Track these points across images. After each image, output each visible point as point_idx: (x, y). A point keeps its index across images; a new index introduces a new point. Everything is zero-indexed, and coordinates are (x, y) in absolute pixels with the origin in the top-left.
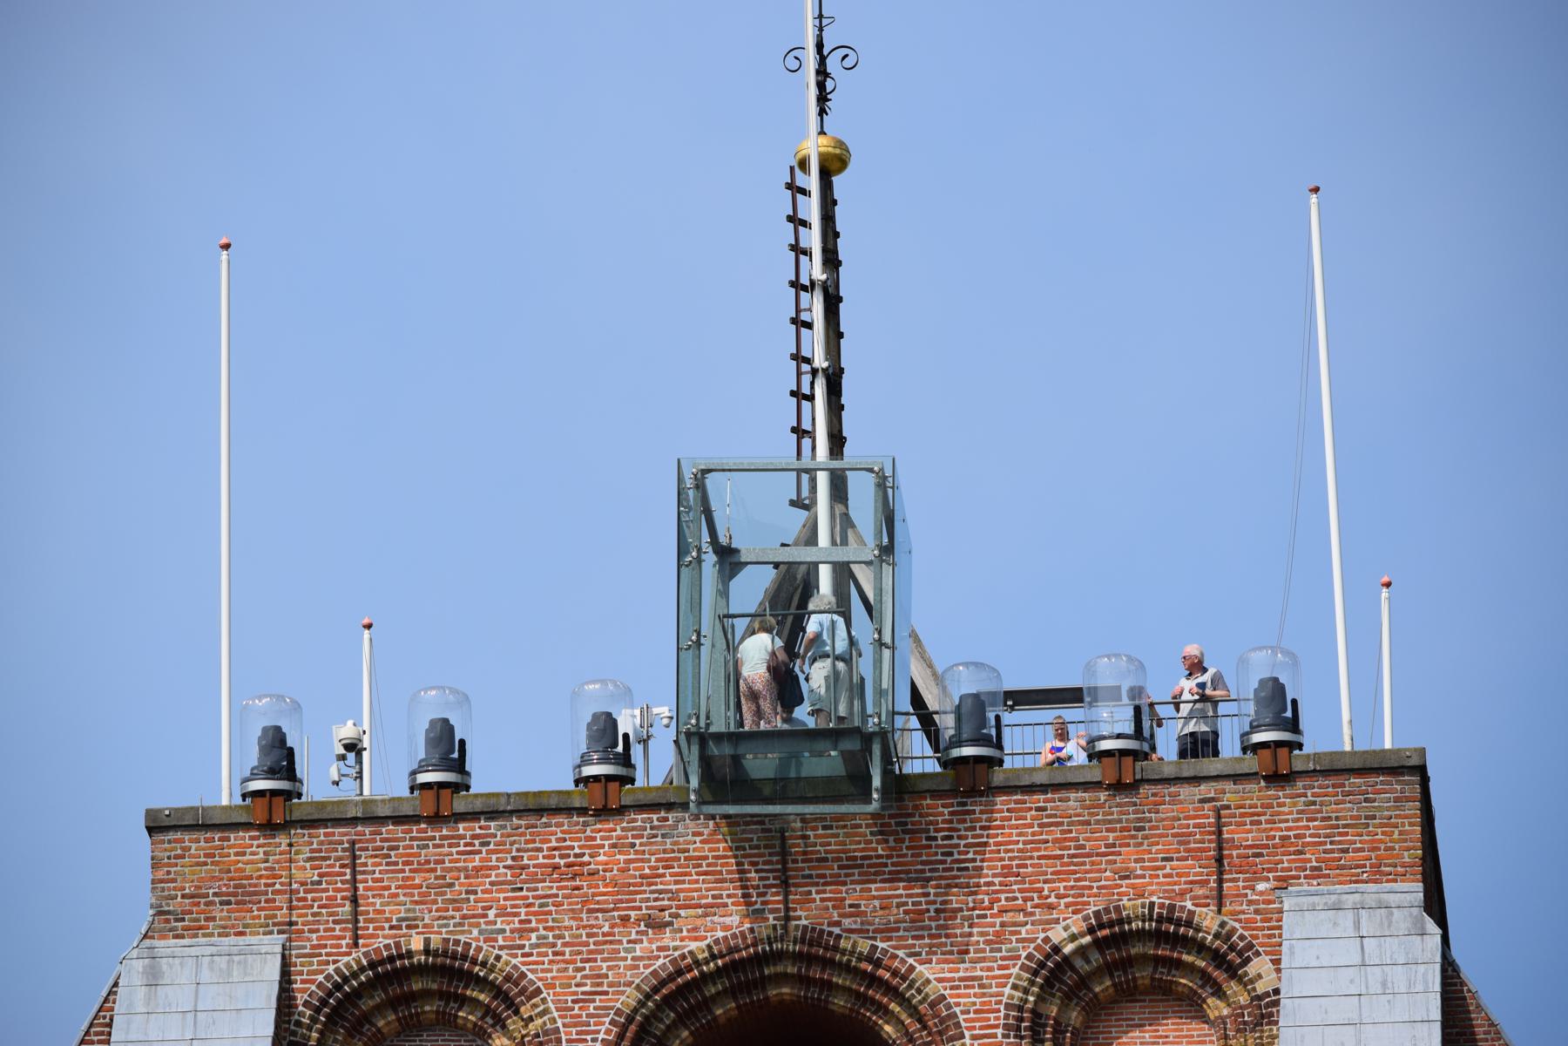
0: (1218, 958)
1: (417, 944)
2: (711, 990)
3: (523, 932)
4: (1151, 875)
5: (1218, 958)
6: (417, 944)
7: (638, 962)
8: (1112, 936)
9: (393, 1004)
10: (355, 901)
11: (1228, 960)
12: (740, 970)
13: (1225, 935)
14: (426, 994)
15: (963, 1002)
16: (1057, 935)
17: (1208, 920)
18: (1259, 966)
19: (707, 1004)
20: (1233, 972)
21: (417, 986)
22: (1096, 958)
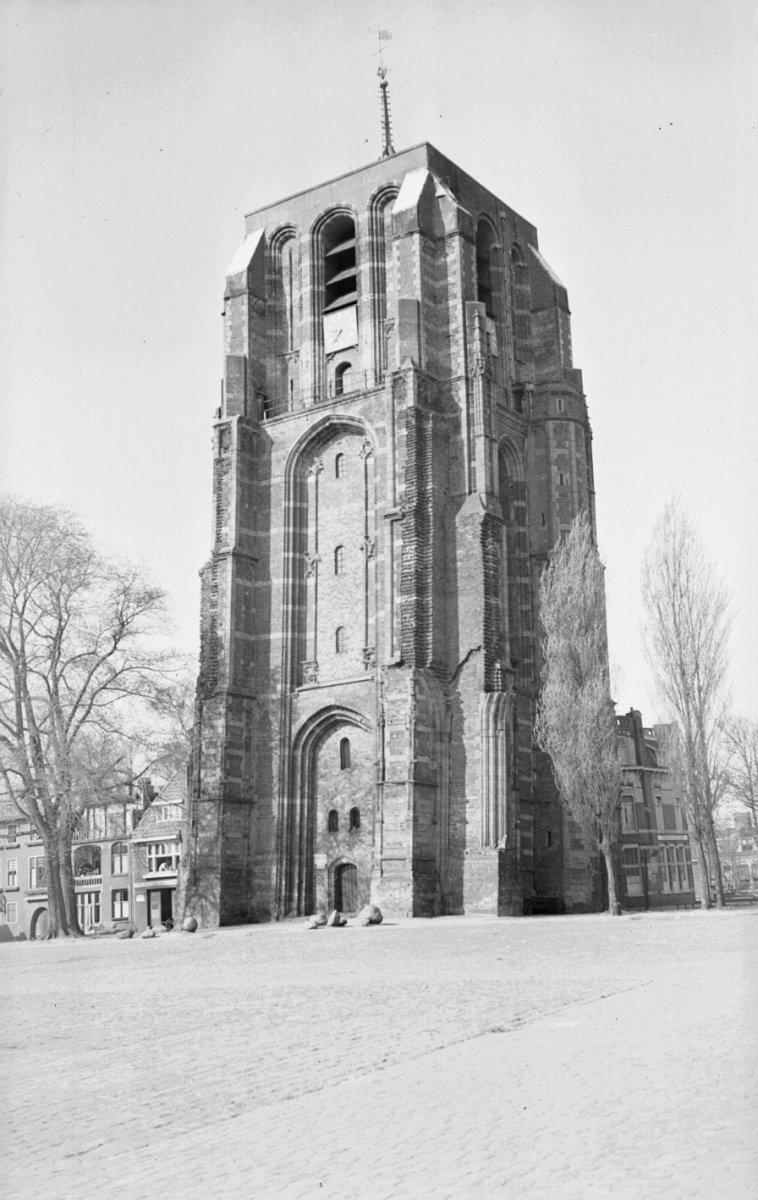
12: (329, 213)
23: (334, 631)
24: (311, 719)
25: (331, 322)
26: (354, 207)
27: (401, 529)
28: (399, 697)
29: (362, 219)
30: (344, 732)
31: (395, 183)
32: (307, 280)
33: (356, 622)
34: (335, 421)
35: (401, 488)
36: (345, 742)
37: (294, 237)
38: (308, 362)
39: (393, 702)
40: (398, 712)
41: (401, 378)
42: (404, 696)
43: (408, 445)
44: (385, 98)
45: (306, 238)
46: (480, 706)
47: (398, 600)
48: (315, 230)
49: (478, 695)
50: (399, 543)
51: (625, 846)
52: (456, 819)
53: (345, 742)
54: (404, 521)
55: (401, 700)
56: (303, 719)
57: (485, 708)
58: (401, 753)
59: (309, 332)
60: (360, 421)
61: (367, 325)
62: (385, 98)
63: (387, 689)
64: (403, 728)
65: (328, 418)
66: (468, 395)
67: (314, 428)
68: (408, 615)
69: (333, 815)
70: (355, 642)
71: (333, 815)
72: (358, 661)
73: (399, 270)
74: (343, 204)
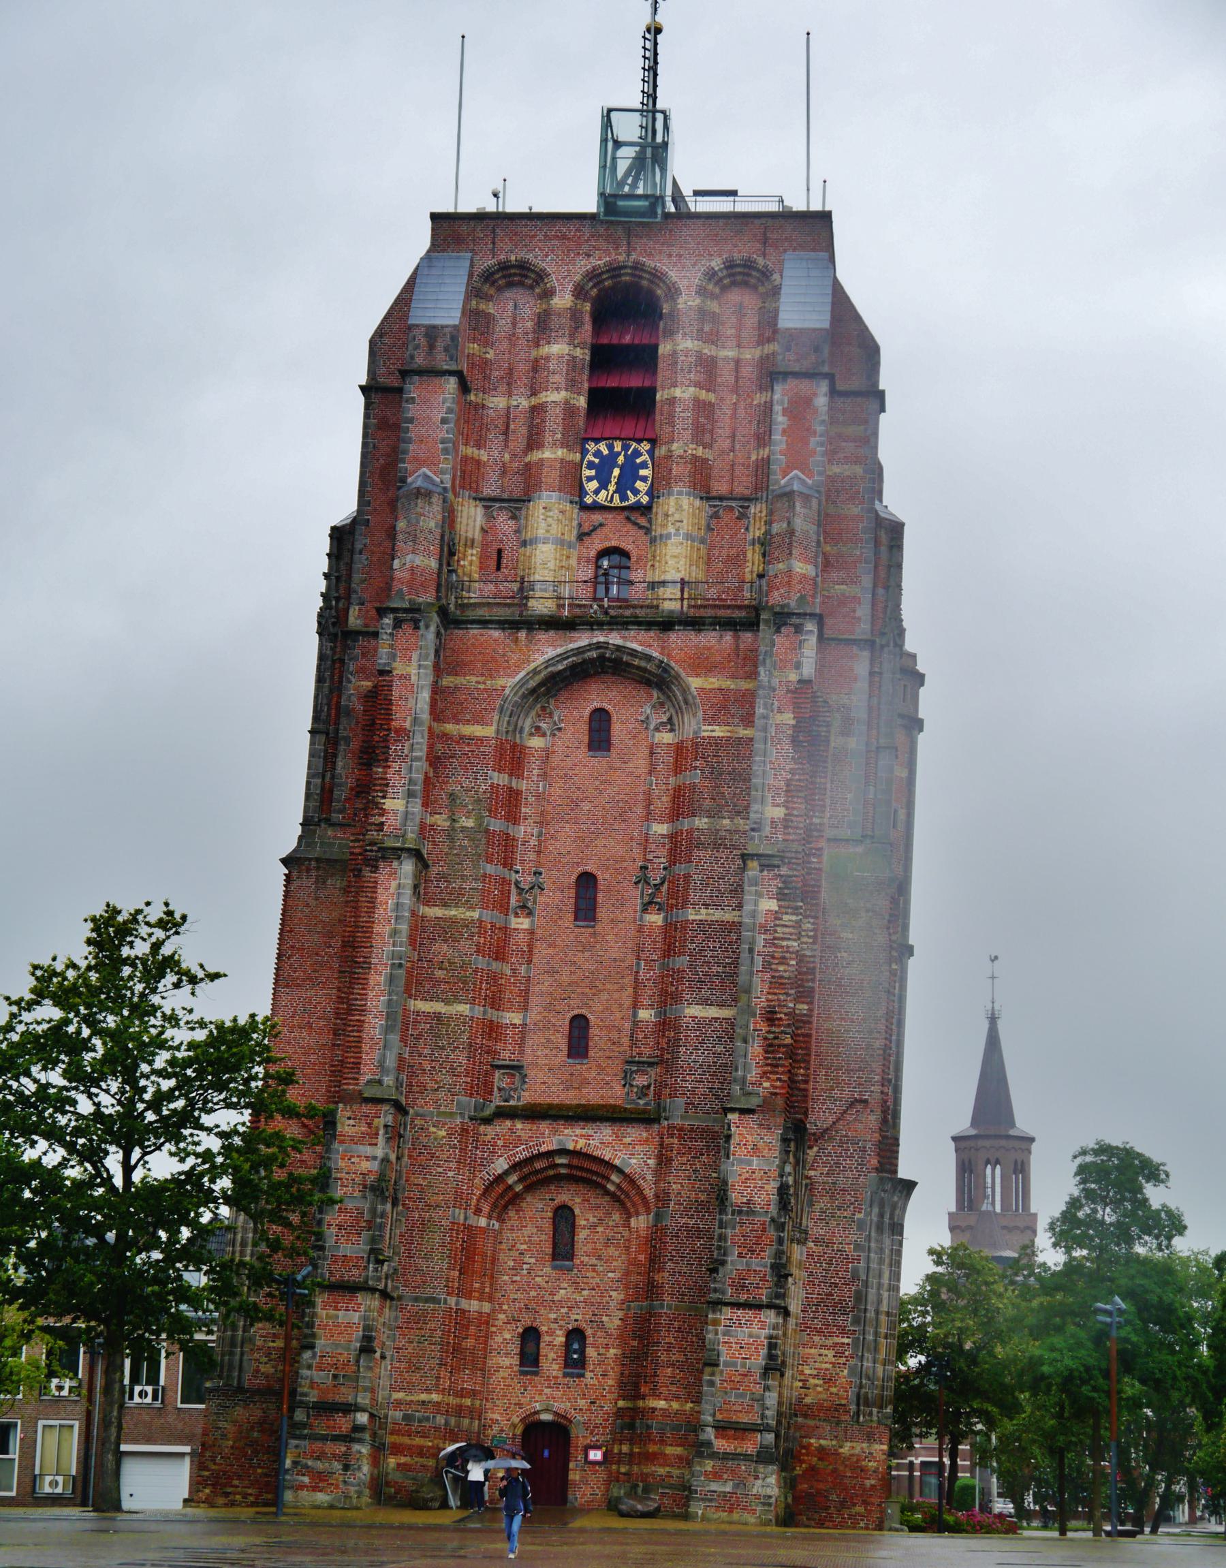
0: (763, 273)
1: (513, 258)
2: (605, 276)
3: (547, 256)
4: (744, 248)
5: (763, 273)
6: (513, 258)
7: (583, 265)
8: (730, 265)
9: (504, 277)
10: (494, 243)
11: (766, 274)
12: (615, 270)
13: (766, 266)
14: (515, 274)
15: (682, 285)
16: (713, 264)
17: (761, 261)
18: (776, 276)
19: (603, 281)
20: (767, 277)
21: (513, 271)
22: (725, 272)
24: (515, 1167)
29: (688, 301)
30: (564, 1196)
36: (563, 1218)
43: (795, 741)
45: (563, 300)
48: (579, 292)
50: (773, 905)
52: (807, 1372)
53: (563, 1218)
56: (501, 1165)
59: (551, 476)
66: (872, 674)
69: (530, 1336)
71: (530, 1336)
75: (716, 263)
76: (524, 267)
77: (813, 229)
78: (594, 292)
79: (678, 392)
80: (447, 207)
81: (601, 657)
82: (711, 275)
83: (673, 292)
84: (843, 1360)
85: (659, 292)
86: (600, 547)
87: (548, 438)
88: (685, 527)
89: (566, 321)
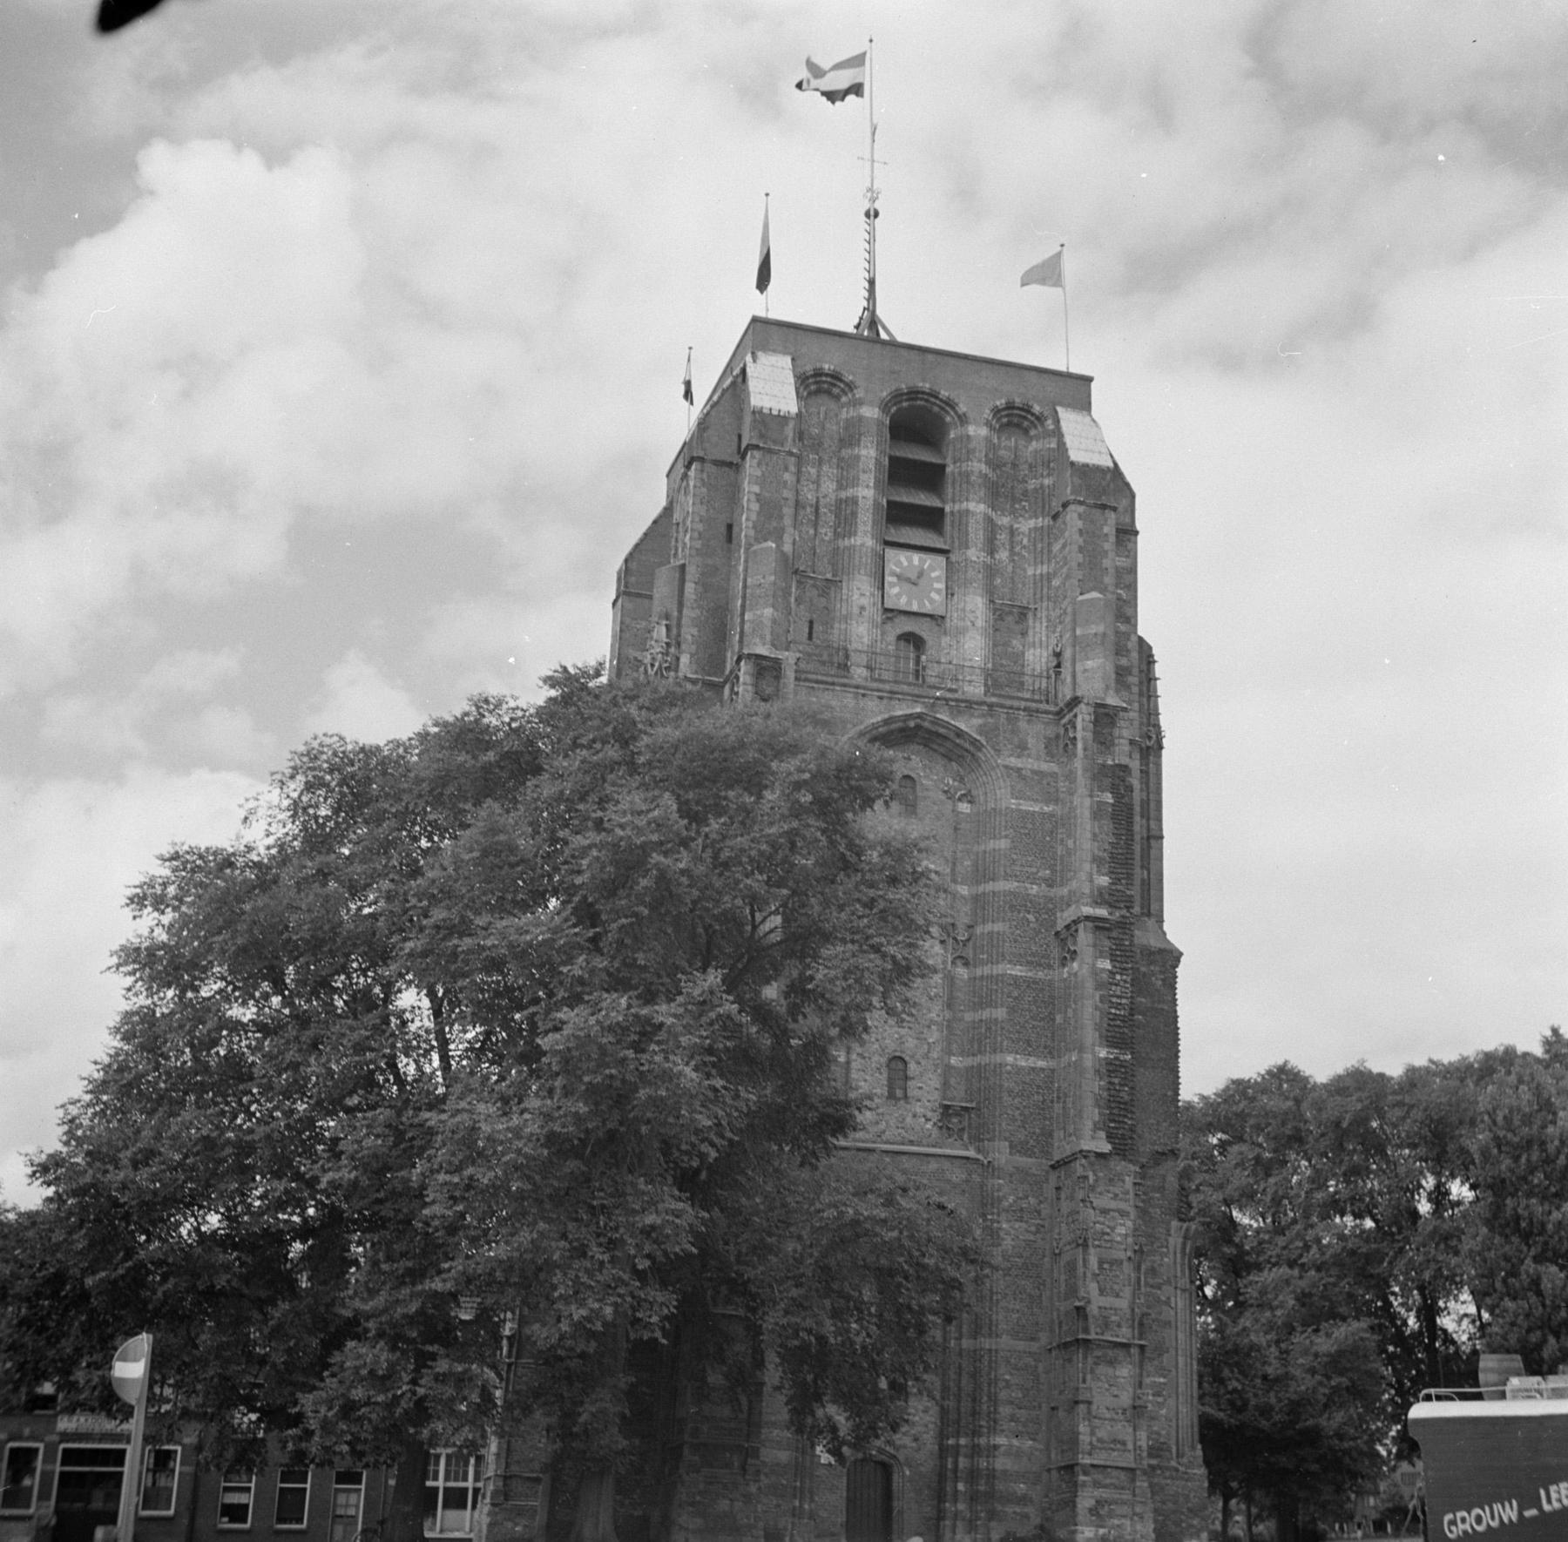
0: (1038, 418)
6: (826, 366)
12: (914, 394)
23: (883, 1060)
25: (900, 561)
26: (962, 408)
27: (1107, 943)
28: (1113, 1205)
31: (1037, 409)
32: (869, 479)
33: (926, 1056)
34: (926, 724)
35: (1104, 881)
37: (837, 398)
38: (862, 608)
39: (1105, 1212)
40: (1113, 1229)
41: (1107, 715)
42: (1122, 1206)
44: (871, 241)
45: (871, 412)
46: (1171, 1240)
47: (1103, 1054)
49: (1168, 1223)
51: (472, 1461)
54: (1114, 934)
55: (1118, 1211)
57: (1179, 1246)
58: (1117, 1296)
60: (974, 742)
61: (975, 604)
62: (871, 241)
63: (1092, 1188)
64: (1122, 1255)
65: (919, 716)
67: (886, 722)
68: (1116, 1081)
70: (926, 1088)
72: (928, 1120)
73: (1081, 550)
74: (944, 394)
75: (1001, 403)
76: (836, 376)
77: (1076, 389)
78: (894, 409)
79: (972, 506)
80: (762, 314)
81: (918, 727)
82: (996, 411)
83: (963, 419)
84: (1160, 1399)
85: (948, 419)
86: (899, 631)
87: (861, 528)
88: (980, 623)
89: (874, 429)
